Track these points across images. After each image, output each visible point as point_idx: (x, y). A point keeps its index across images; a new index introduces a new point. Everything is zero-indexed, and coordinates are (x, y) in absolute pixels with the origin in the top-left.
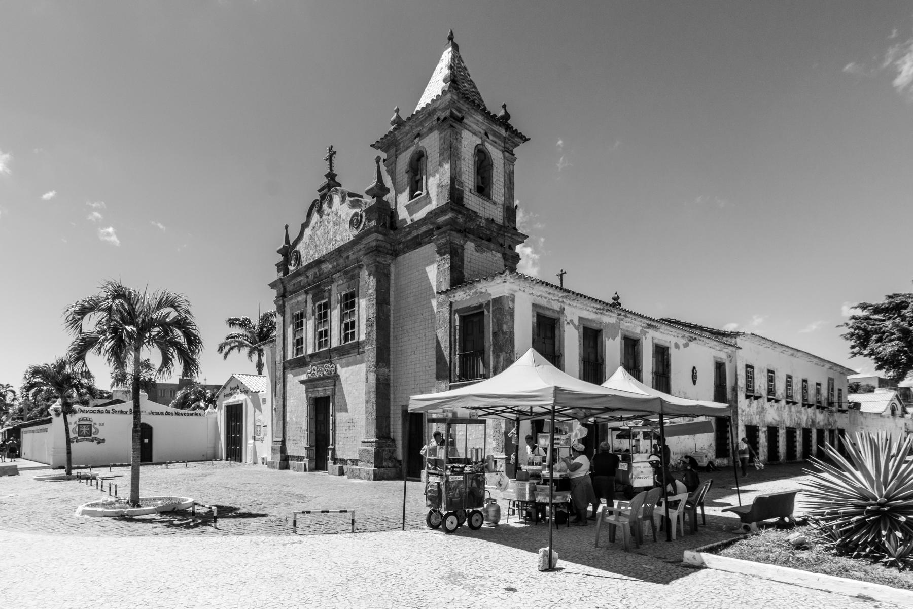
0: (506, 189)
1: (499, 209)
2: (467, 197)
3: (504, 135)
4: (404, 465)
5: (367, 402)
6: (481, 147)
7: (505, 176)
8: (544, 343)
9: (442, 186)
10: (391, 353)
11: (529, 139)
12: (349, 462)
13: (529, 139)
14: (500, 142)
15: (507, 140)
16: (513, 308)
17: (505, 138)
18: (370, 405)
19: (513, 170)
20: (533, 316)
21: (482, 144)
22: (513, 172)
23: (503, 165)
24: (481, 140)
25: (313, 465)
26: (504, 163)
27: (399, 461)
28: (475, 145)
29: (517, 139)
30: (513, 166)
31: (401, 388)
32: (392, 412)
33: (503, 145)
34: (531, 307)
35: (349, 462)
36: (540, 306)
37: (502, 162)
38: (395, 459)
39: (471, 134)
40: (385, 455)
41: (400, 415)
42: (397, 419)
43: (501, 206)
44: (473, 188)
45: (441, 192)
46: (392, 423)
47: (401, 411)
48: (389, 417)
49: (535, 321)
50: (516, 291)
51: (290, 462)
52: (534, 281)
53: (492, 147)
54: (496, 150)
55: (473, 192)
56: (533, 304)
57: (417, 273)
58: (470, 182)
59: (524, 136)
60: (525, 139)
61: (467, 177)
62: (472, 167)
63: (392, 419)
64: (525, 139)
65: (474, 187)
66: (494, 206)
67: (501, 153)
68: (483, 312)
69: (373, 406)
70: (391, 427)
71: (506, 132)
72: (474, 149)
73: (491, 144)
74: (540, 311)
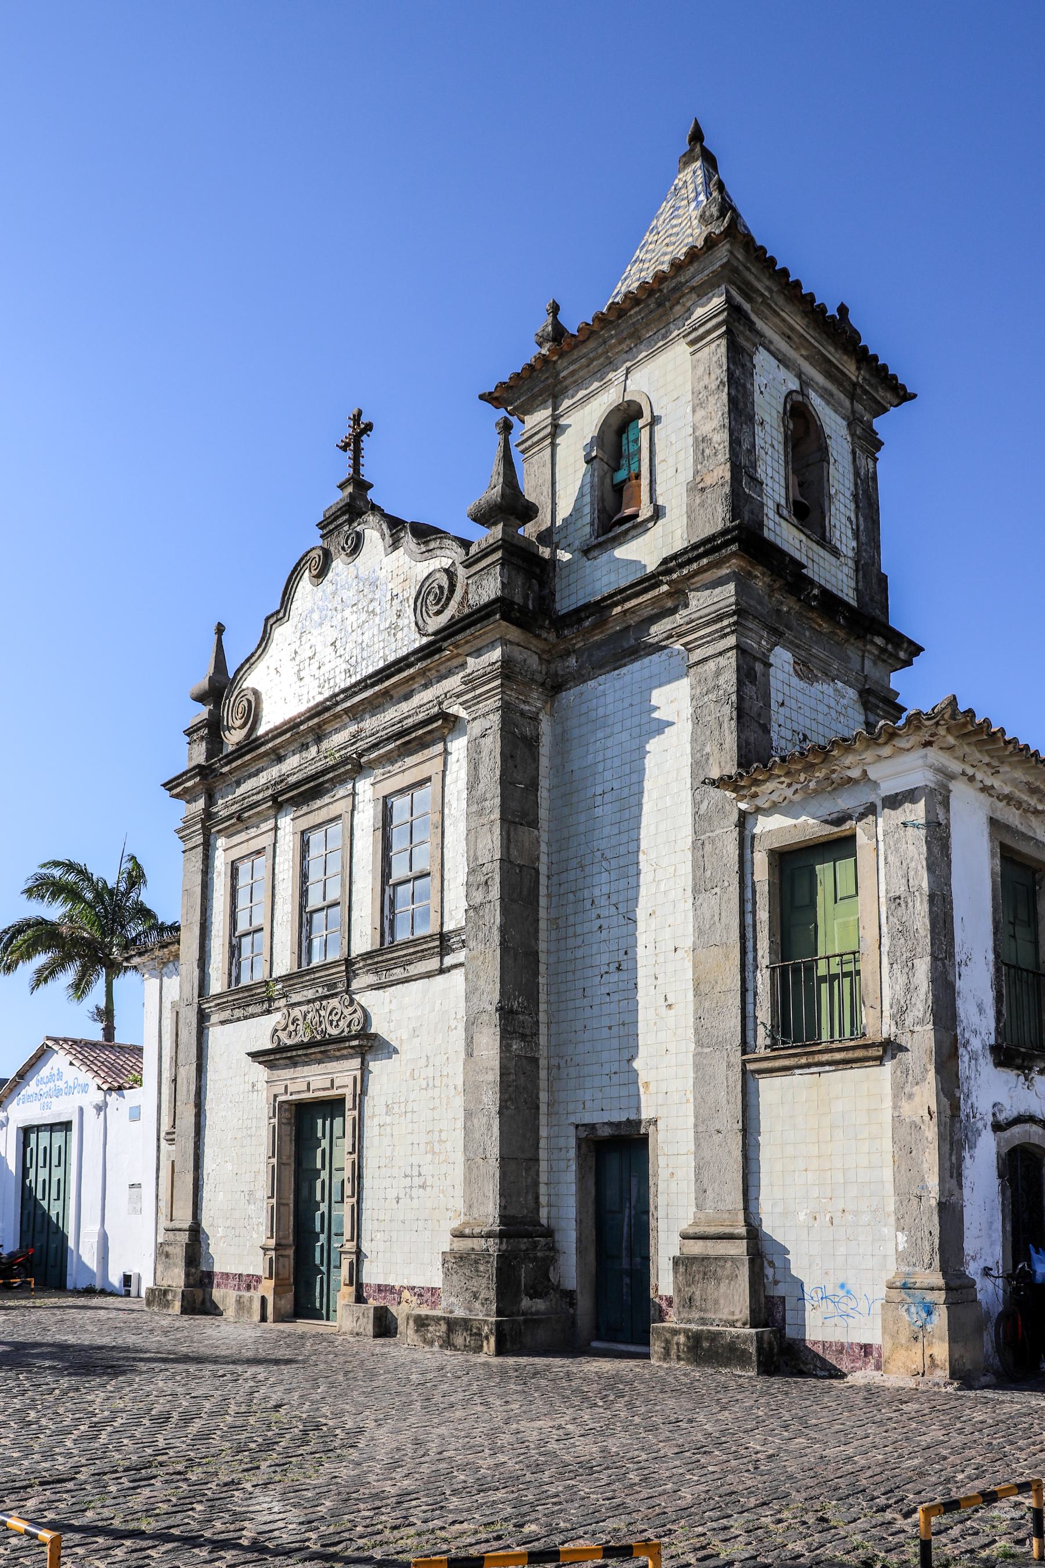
0: (861, 519)
1: (846, 569)
2: (771, 525)
3: (854, 378)
4: (584, 1304)
5: (469, 1114)
6: (800, 398)
7: (856, 484)
8: (1014, 937)
9: (703, 490)
10: (542, 968)
11: (914, 396)
12: (406, 1294)
13: (914, 396)
14: (842, 396)
15: (859, 391)
16: (948, 826)
17: (855, 385)
18: (479, 1122)
19: (875, 473)
20: (993, 855)
21: (802, 392)
22: (874, 478)
23: (850, 457)
24: (797, 382)
25: (288, 1302)
26: (854, 453)
27: (570, 1295)
28: (784, 391)
29: (882, 395)
30: (875, 460)
31: (573, 1073)
32: (543, 1143)
33: (847, 403)
34: (985, 829)
35: (406, 1294)
36: (1007, 828)
37: (848, 447)
38: (557, 1288)
39: (774, 363)
40: (524, 1273)
41: (572, 1153)
42: (563, 1164)
43: (851, 563)
44: (783, 502)
45: (702, 505)
46: (543, 1178)
47: (573, 1142)
48: (537, 1160)
49: (998, 869)
50: (951, 777)
51: (214, 1290)
52: (1011, 747)
53: (823, 403)
54: (833, 414)
55: (785, 513)
56: (991, 818)
57: (625, 736)
58: (776, 487)
59: (903, 387)
60: (903, 395)
61: (769, 471)
62: (781, 448)
63: (543, 1166)
64: (903, 395)
65: (787, 499)
66: (833, 559)
67: (845, 423)
68: (852, 838)
69: (489, 1127)
70: (543, 1189)
71: (859, 369)
72: (782, 400)
73: (821, 396)
74: (1009, 841)
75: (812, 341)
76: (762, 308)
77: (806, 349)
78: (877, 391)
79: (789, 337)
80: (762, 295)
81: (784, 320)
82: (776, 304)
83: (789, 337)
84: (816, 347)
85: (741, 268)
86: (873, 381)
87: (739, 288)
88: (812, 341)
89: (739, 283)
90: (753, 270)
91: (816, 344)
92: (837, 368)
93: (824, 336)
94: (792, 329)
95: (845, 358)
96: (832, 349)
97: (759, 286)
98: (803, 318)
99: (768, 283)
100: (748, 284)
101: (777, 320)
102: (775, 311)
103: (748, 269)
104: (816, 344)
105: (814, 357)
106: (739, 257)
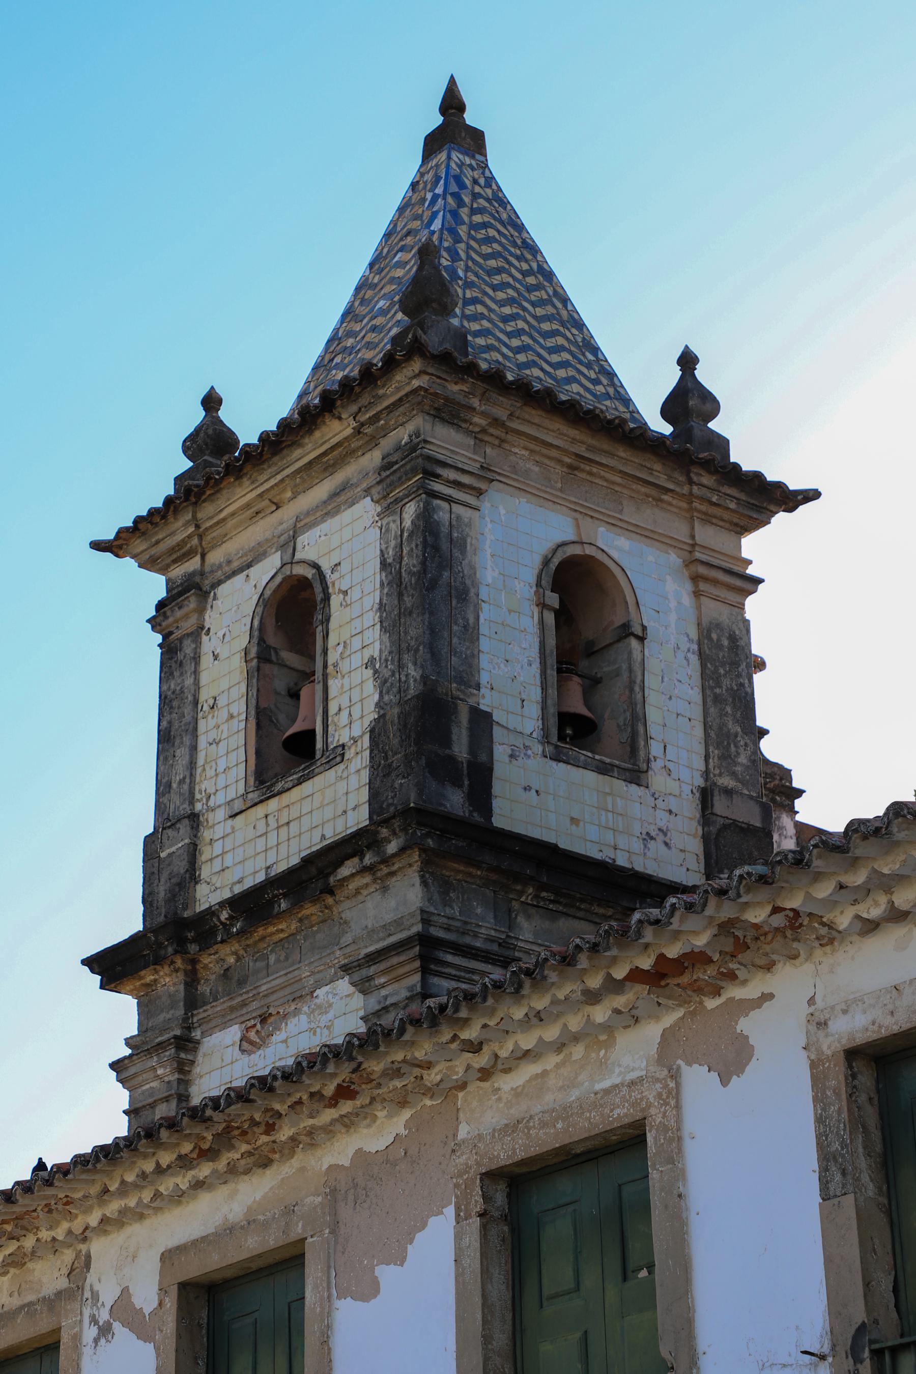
3: (349, 431)
75: (272, 482)
76: (209, 538)
77: (284, 490)
78: (384, 396)
79: (257, 513)
80: (190, 537)
81: (233, 514)
82: (211, 518)
83: (257, 513)
84: (282, 481)
85: (154, 551)
86: (365, 400)
87: (175, 561)
88: (272, 482)
89: (169, 560)
90: (160, 536)
91: (279, 477)
92: (324, 454)
93: (275, 459)
94: (248, 506)
95: (317, 434)
96: (298, 452)
97: (179, 537)
98: (240, 485)
99: (180, 523)
100: (172, 550)
101: (231, 523)
102: (218, 523)
103: (158, 542)
104: (279, 477)
105: (296, 486)
106: (141, 548)
